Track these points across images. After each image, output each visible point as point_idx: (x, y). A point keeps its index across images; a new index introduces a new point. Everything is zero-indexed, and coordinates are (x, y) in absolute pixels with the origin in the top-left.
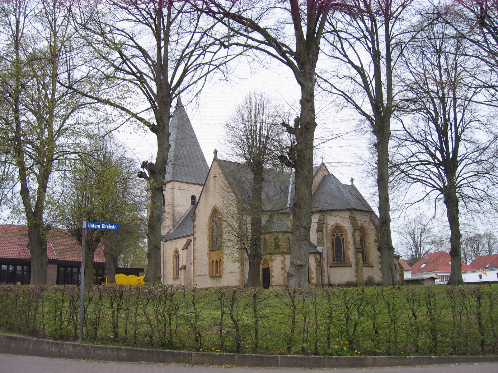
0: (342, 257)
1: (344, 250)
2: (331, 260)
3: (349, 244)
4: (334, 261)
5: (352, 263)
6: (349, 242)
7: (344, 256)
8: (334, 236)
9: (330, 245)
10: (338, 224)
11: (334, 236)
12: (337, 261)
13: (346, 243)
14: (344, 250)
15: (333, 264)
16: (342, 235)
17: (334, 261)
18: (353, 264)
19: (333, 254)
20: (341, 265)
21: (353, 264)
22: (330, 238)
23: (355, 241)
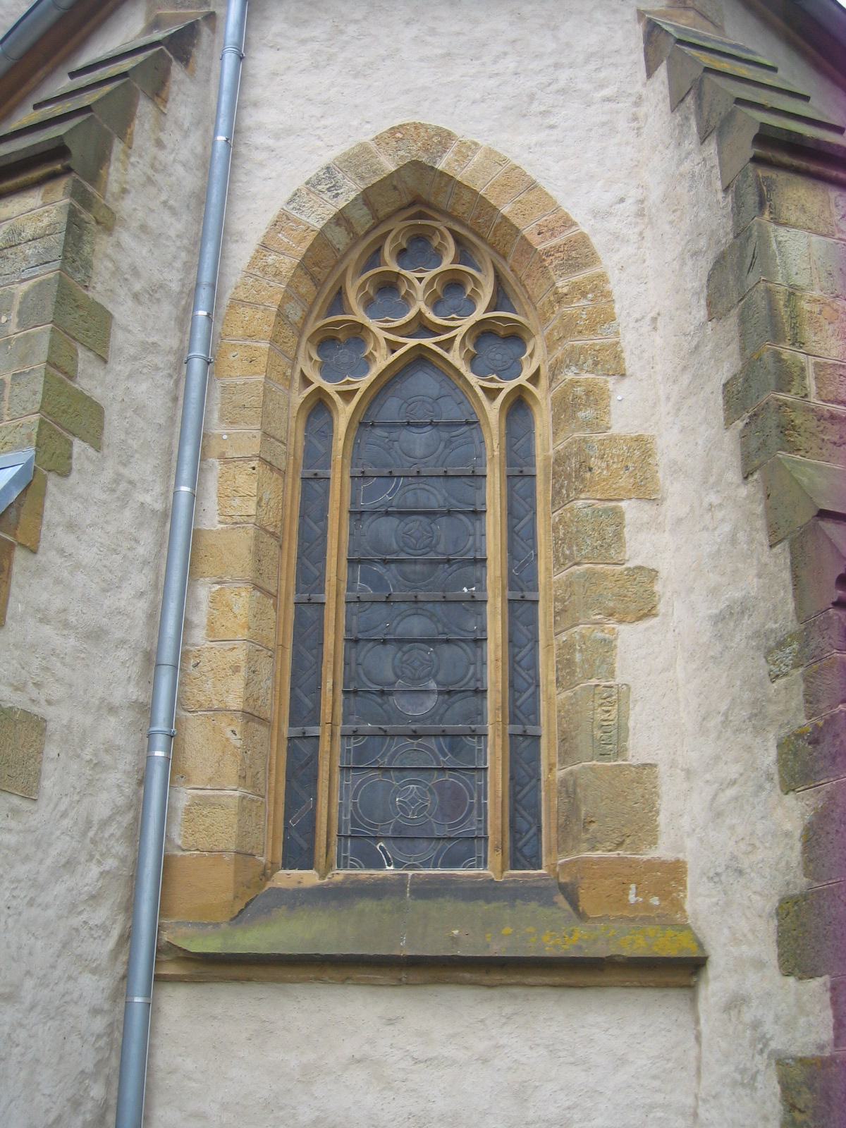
0: (463, 740)
1: (519, 475)
2: (219, 802)
3: (646, 491)
4: (298, 852)
5: (699, 902)
6: (642, 447)
7: (523, 747)
8: (339, 343)
9: (237, 501)
10: (444, 138)
11: (339, 343)
12: (360, 844)
13: (574, 470)
14: (521, 607)
15: (255, 902)
16: (500, 339)
17: (298, 852)
18: (733, 923)
19: (303, 709)
20: (455, 932)
21: (733, 923)
22: (257, 375)
23: (786, 377)
